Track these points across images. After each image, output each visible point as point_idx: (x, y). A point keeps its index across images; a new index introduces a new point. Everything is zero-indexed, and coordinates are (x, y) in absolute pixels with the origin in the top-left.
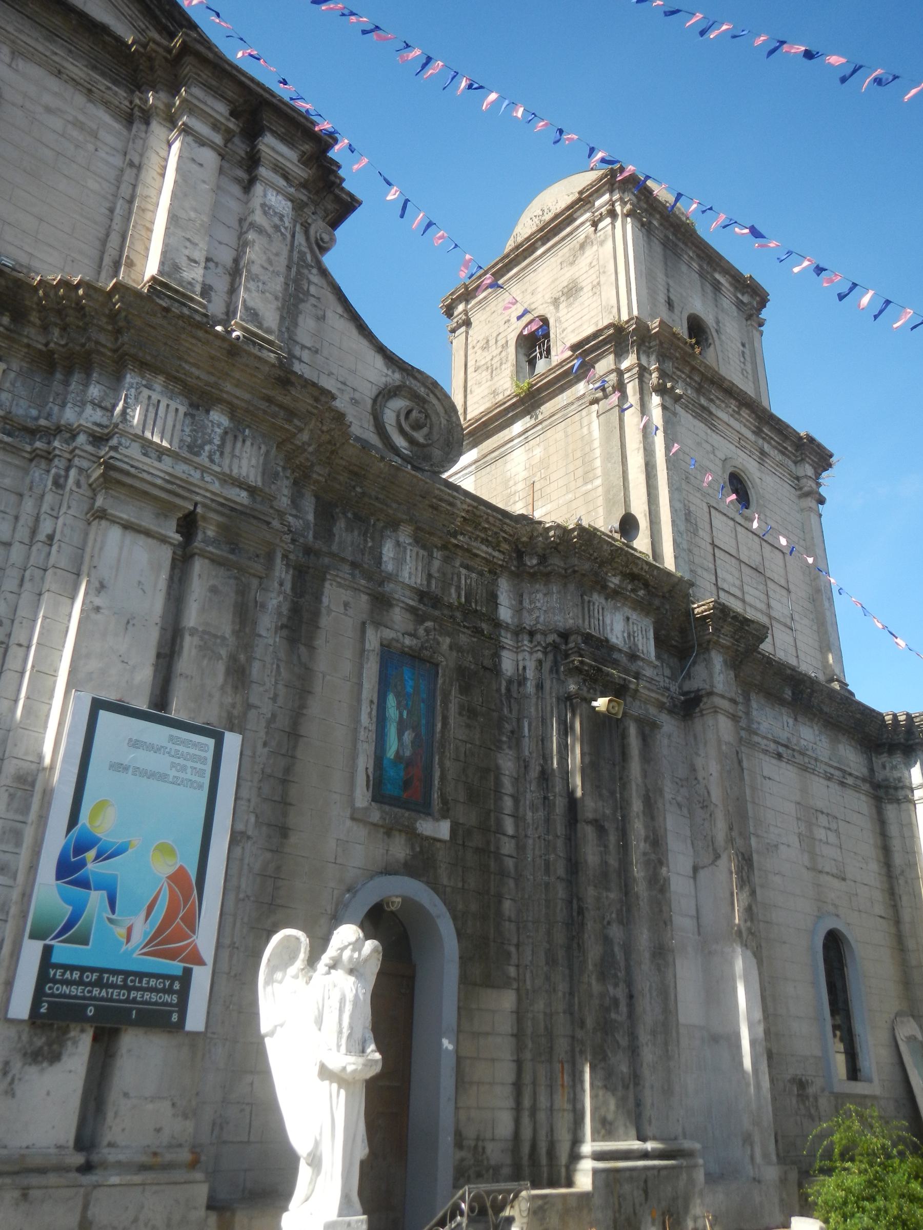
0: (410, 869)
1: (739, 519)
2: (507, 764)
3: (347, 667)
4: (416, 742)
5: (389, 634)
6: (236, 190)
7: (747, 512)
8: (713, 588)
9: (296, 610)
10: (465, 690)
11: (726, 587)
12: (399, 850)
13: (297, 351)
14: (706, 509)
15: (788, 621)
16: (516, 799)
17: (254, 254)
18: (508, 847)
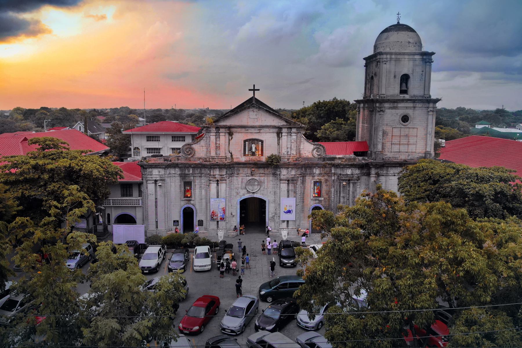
0: (318, 203)
1: (402, 126)
2: (333, 190)
3: (309, 185)
4: (319, 190)
5: (314, 180)
6: (290, 136)
7: (406, 123)
8: (391, 145)
9: (303, 181)
10: (326, 183)
11: (395, 143)
12: (317, 201)
13: (301, 150)
14: (391, 128)
15: (415, 143)
16: (334, 193)
17: (292, 146)
18: (333, 199)
